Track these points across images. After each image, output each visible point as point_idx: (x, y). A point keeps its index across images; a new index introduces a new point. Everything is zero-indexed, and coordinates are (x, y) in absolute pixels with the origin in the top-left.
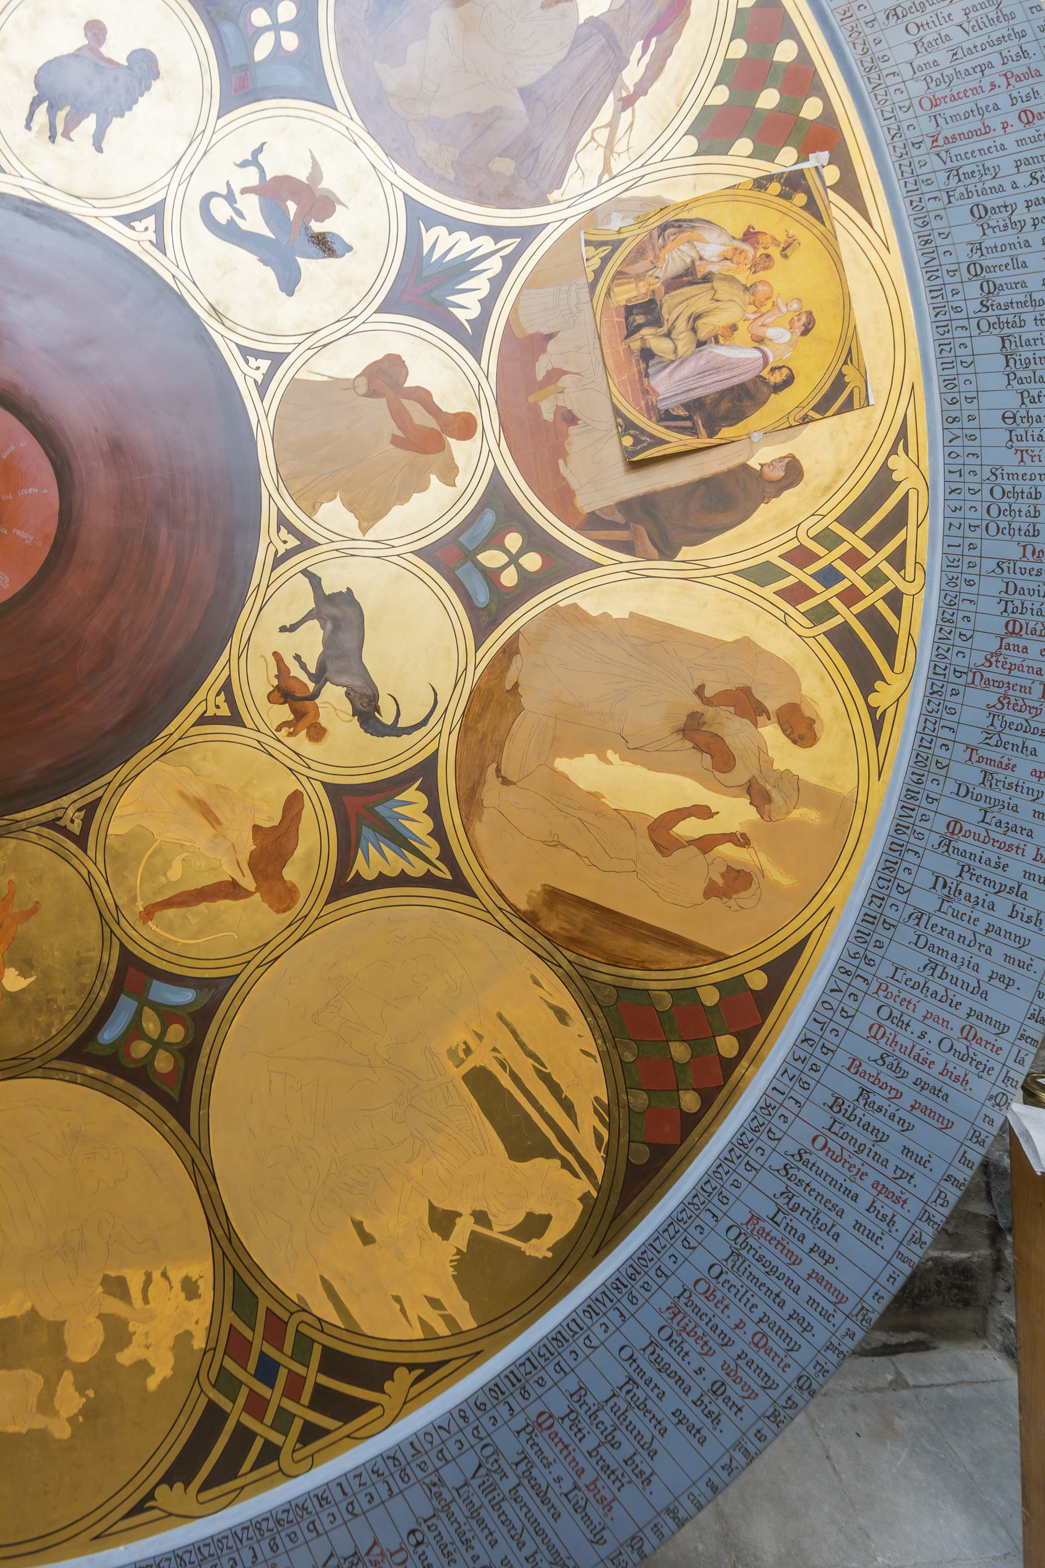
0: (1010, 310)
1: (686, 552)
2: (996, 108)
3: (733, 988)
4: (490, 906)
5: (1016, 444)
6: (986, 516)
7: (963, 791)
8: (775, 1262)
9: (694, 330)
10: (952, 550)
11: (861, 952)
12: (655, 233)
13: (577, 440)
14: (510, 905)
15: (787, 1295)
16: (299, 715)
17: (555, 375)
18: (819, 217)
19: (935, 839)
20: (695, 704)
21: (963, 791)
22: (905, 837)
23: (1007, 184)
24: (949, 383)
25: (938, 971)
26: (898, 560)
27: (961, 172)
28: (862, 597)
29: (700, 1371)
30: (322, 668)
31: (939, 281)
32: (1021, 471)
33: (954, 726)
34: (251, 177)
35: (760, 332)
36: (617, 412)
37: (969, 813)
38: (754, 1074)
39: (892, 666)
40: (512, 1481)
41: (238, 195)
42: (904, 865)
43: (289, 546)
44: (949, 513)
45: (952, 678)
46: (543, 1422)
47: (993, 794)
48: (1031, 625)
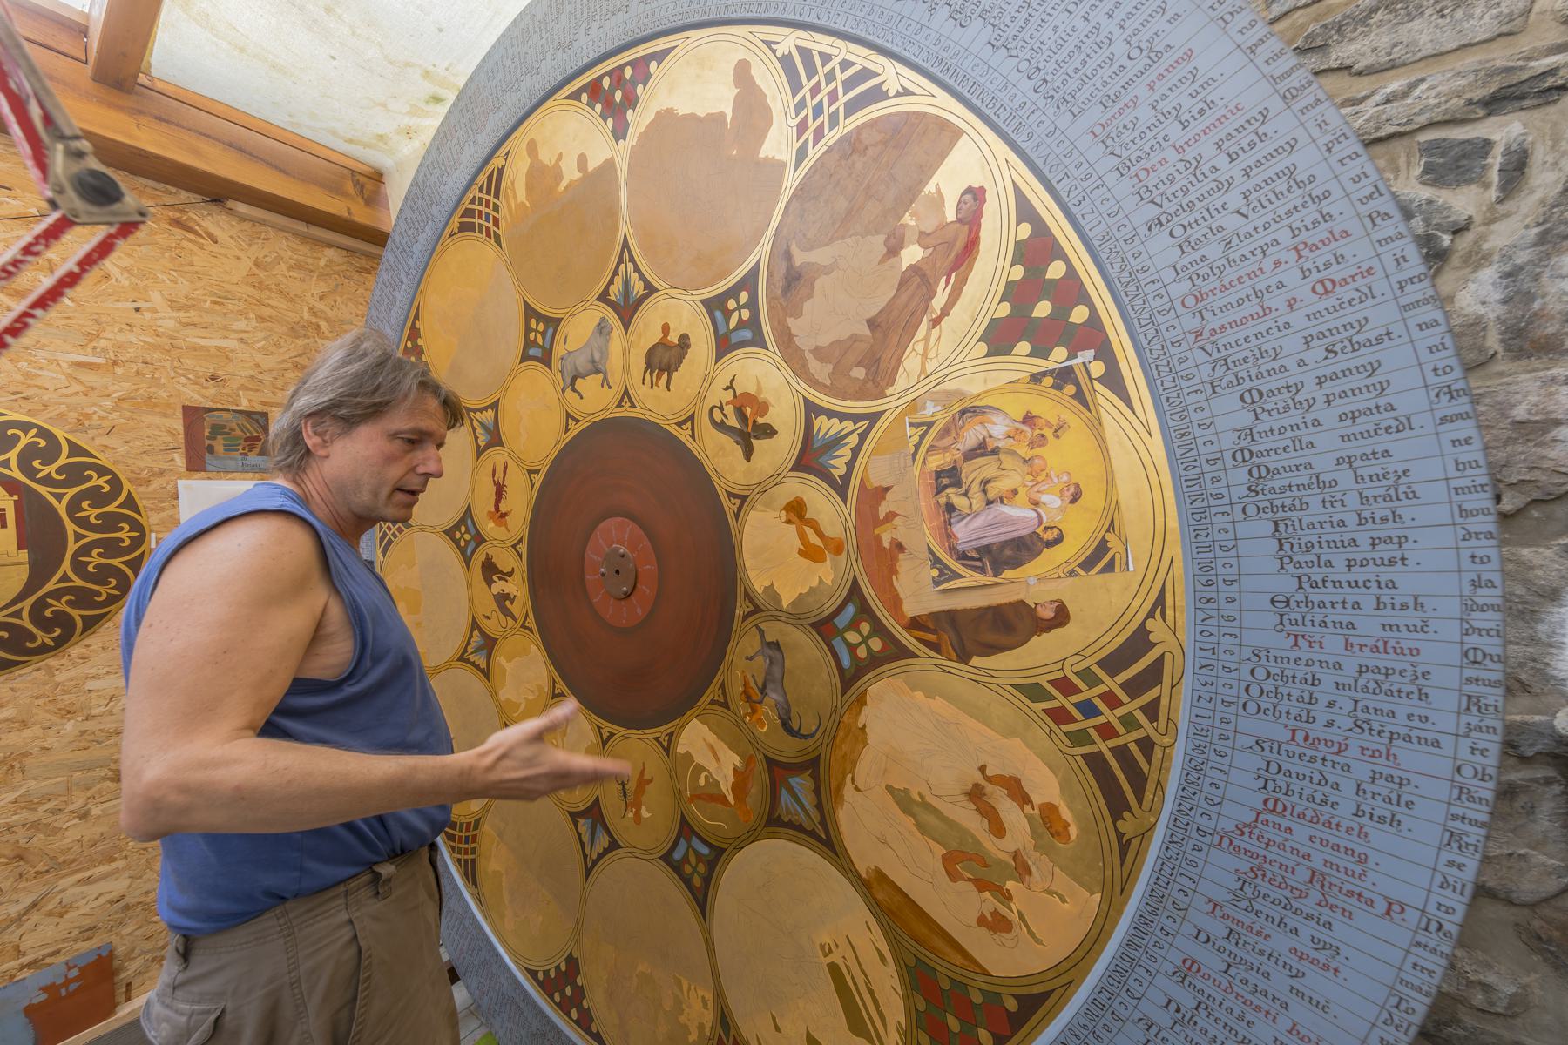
0: (1288, 494)
1: (976, 661)
2: (1280, 285)
5: (1288, 627)
7: (1203, 937)
9: (985, 491)
10: (1199, 720)
13: (903, 564)
17: (891, 516)
18: (1087, 406)
19: (1171, 970)
23: (1291, 363)
24: (1207, 566)
26: (1152, 710)
27: (1229, 360)
30: (764, 687)
31: (1197, 470)
32: (1293, 655)
34: (729, 395)
35: (1036, 497)
37: (1212, 962)
39: (1140, 801)
44: (1198, 686)
45: (1194, 834)
47: (1240, 953)
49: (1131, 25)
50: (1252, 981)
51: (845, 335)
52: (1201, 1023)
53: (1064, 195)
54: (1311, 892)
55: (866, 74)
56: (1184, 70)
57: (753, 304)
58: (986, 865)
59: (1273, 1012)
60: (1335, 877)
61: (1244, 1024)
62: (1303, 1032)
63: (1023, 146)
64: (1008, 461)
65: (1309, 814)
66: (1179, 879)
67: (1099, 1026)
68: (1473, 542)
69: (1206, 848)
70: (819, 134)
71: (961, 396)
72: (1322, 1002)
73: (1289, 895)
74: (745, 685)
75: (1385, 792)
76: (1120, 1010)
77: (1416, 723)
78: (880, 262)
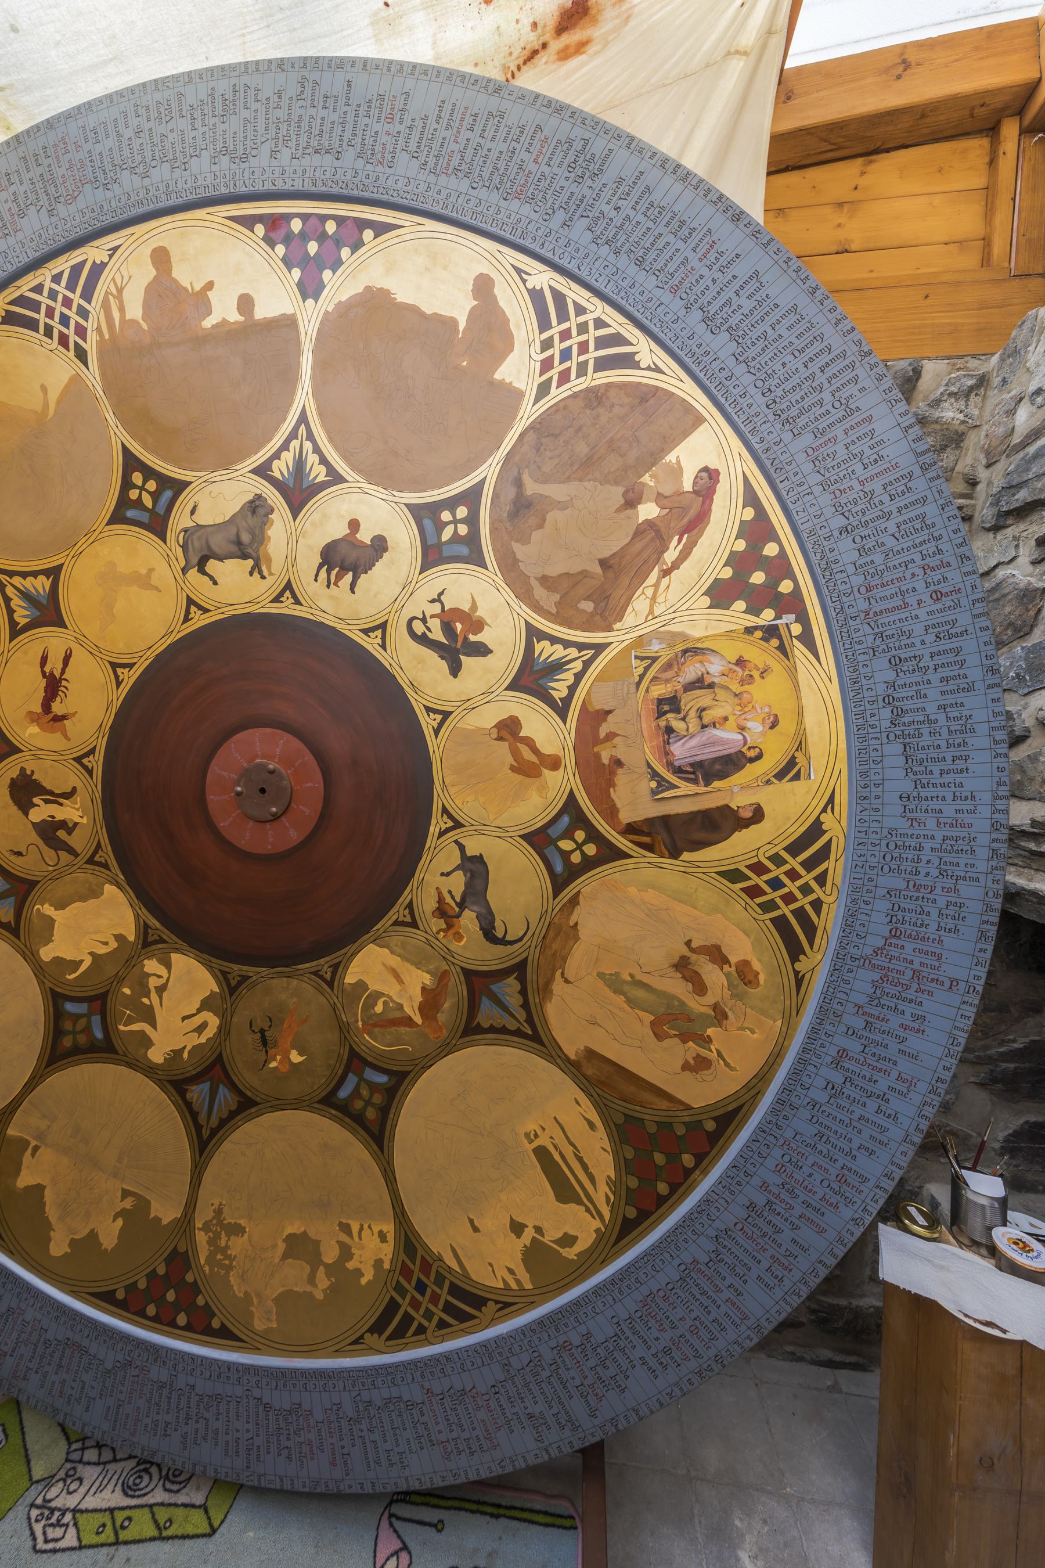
0: (912, 727)
1: (686, 856)
2: (914, 590)
4: (553, 1053)
5: (908, 814)
6: (882, 860)
7: (850, 1032)
8: (706, 1289)
9: (700, 718)
10: (856, 881)
12: (680, 654)
13: (621, 778)
14: (565, 1055)
15: (712, 1308)
16: (450, 926)
17: (611, 736)
19: (829, 1059)
21: (851, 1032)
22: (809, 1056)
24: (865, 774)
25: (824, 1139)
26: (821, 880)
28: (796, 900)
29: (657, 1339)
31: (862, 708)
33: (848, 991)
34: (436, 608)
35: (743, 723)
37: (854, 1046)
38: (702, 1180)
39: (811, 947)
40: (547, 1373)
41: (428, 619)
42: (806, 1072)
43: (448, 826)
44: (855, 857)
45: (849, 962)
46: (566, 1346)
47: (871, 1036)
48: (909, 932)
49: (836, 383)
51: (575, 569)
53: (784, 493)
55: (617, 339)
56: (866, 428)
57: (472, 521)
58: (690, 1020)
63: (757, 446)
64: (721, 694)
65: (914, 934)
68: (999, 759)
69: (855, 969)
70: (564, 377)
71: (684, 637)
74: (441, 900)
77: (969, 869)
78: (618, 511)
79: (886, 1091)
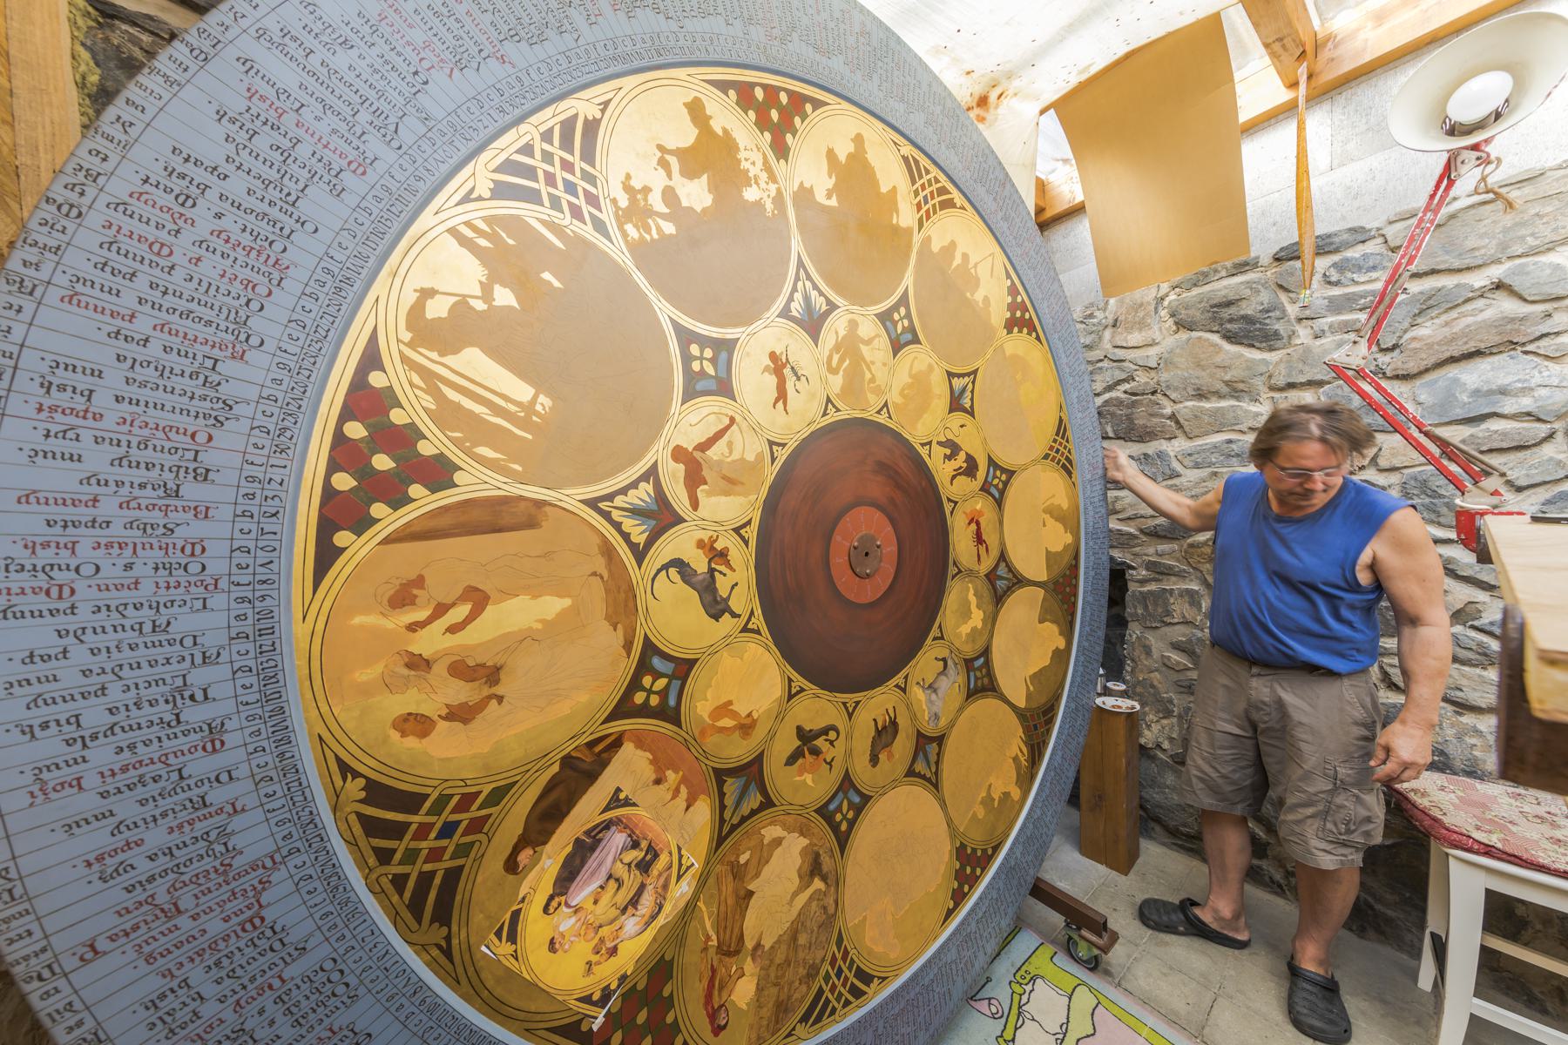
1: (556, 768)
3: (362, 524)
7: (224, 777)
9: (617, 880)
11: (257, 604)
13: (649, 773)
16: (712, 548)
17: (677, 792)
19: (229, 725)
20: (499, 690)
25: (147, 628)
30: (713, 577)
36: (635, 805)
37: (200, 766)
44: (381, 939)
45: (298, 844)
47: (182, 796)
48: (233, 939)
50: (152, 785)
52: (162, 706)
54: (168, 897)
59: (109, 780)
60: (159, 926)
61: (124, 744)
62: (68, 791)
65: (222, 945)
66: (283, 801)
67: (250, 613)
72: (75, 830)
73: (184, 878)
74: (728, 564)
75: (178, 1015)
76: (243, 646)
79: (85, 753)
